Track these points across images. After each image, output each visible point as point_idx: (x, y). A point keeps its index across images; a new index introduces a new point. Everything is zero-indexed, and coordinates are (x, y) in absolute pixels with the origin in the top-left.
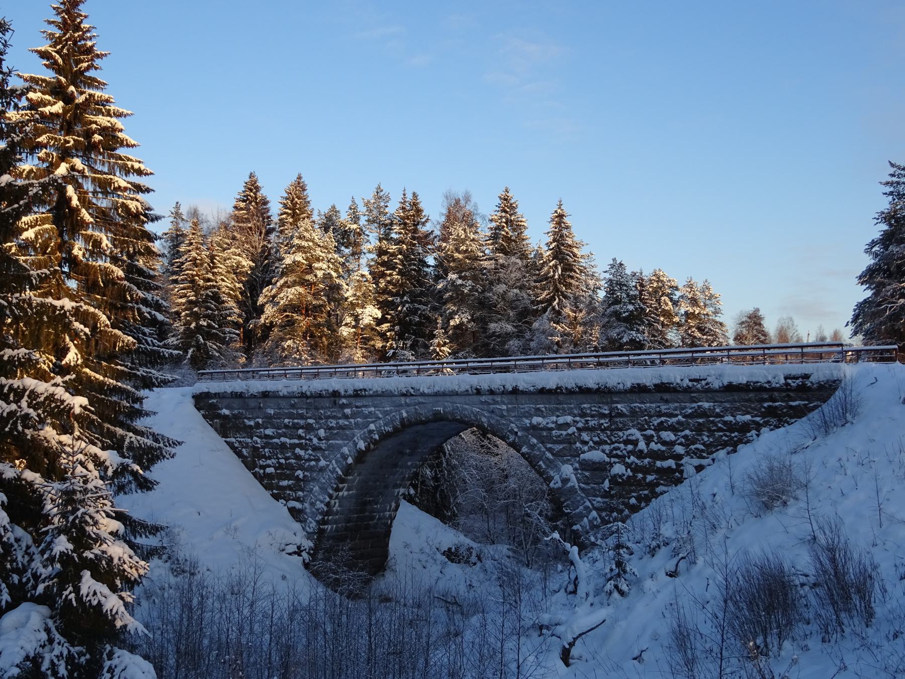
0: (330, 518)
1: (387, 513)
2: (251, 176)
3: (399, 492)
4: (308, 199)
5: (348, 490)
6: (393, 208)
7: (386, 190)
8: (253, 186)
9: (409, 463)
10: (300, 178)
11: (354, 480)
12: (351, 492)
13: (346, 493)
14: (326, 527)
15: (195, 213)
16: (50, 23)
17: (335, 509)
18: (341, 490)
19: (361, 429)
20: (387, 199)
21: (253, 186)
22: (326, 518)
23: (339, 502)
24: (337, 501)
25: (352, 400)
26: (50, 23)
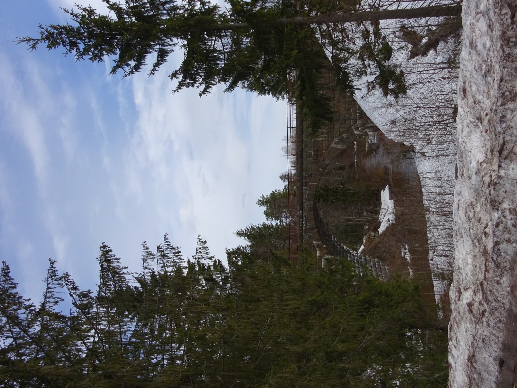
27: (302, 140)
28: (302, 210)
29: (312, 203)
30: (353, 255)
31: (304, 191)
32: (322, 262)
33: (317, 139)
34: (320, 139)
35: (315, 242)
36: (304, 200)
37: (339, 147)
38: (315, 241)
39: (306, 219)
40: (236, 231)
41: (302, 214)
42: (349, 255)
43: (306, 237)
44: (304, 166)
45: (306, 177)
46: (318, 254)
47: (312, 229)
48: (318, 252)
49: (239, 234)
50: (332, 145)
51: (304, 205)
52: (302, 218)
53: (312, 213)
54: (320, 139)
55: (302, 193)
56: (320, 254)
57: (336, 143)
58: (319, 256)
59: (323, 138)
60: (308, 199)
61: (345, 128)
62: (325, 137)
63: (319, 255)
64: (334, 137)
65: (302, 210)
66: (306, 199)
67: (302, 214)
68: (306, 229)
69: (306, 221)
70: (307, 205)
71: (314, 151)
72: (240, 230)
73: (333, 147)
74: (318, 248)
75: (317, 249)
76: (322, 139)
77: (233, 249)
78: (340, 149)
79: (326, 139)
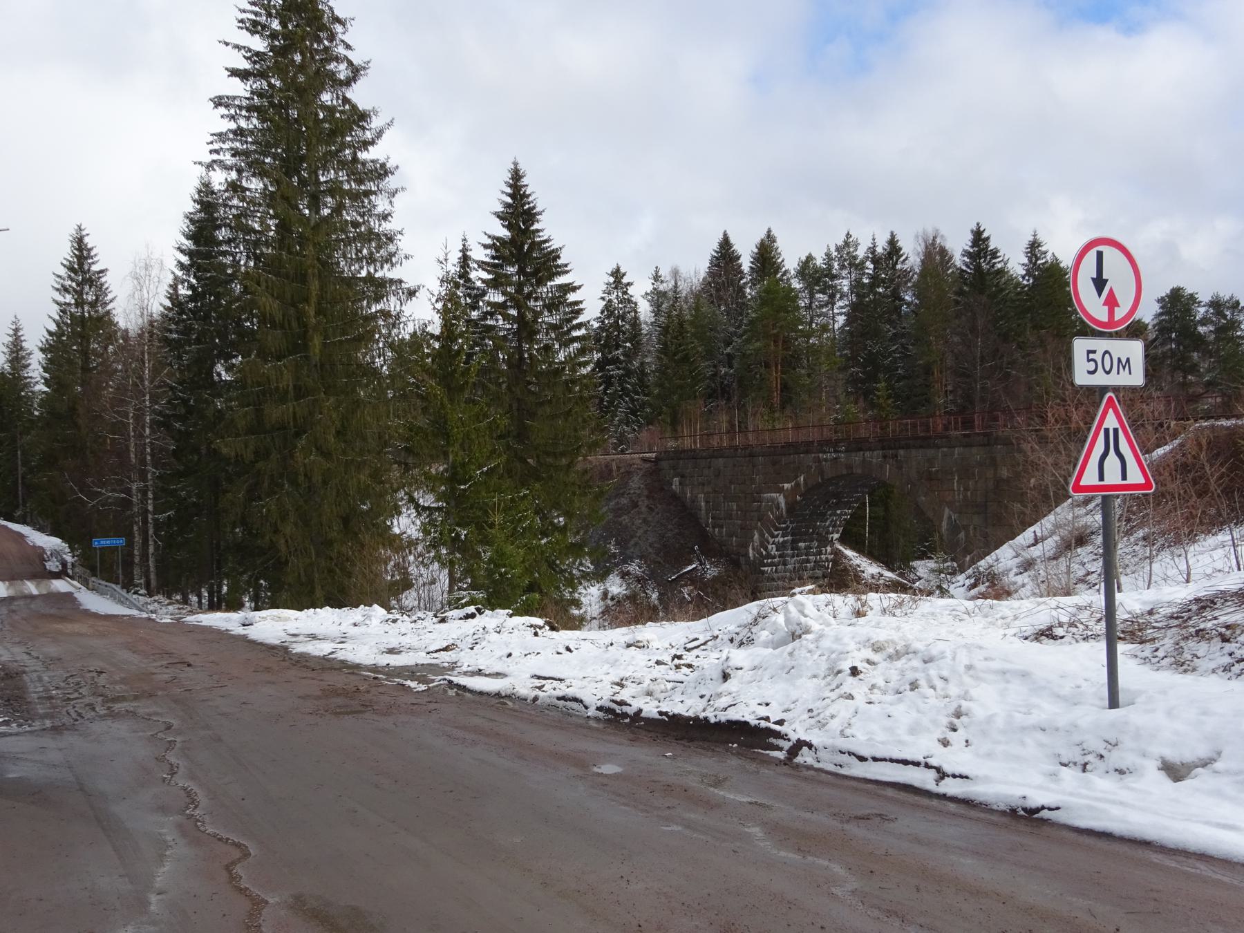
0: (769, 561)
1: (823, 557)
2: (725, 235)
3: (832, 538)
4: (779, 251)
5: (783, 536)
6: (861, 253)
7: (854, 236)
8: (725, 244)
9: (839, 512)
10: (769, 231)
11: (788, 527)
12: (786, 538)
13: (781, 540)
14: (766, 569)
15: (675, 273)
16: (503, 192)
17: (773, 553)
18: (777, 536)
20: (856, 245)
21: (725, 244)
22: (765, 561)
23: (777, 547)
24: (774, 546)
26: (503, 192)
27: (954, 447)
28: (846, 451)
29: (859, 471)
30: (820, 553)
33: (956, 478)
34: (955, 484)
35: (802, 479)
36: (862, 453)
37: (944, 524)
38: (804, 478)
39: (836, 458)
40: (1041, 237)
41: (840, 452)
42: (815, 544)
43: (809, 459)
44: (914, 452)
45: (896, 456)
46: (787, 486)
47: (822, 473)
49: (1034, 246)
50: (947, 511)
51: (853, 454)
52: (836, 451)
53: (845, 472)
54: (955, 484)
55: (873, 451)
56: (787, 489)
57: (950, 517)
59: (959, 490)
61: (975, 536)
62: (959, 495)
63: (785, 488)
64: (960, 513)
65: (846, 451)
66: (864, 458)
67: (840, 452)
68: (819, 461)
69: (831, 460)
70: (855, 460)
71: (937, 471)
72: (1043, 249)
73: (944, 510)
76: (956, 488)
77: (988, 238)
78: (941, 527)
79: (957, 497)
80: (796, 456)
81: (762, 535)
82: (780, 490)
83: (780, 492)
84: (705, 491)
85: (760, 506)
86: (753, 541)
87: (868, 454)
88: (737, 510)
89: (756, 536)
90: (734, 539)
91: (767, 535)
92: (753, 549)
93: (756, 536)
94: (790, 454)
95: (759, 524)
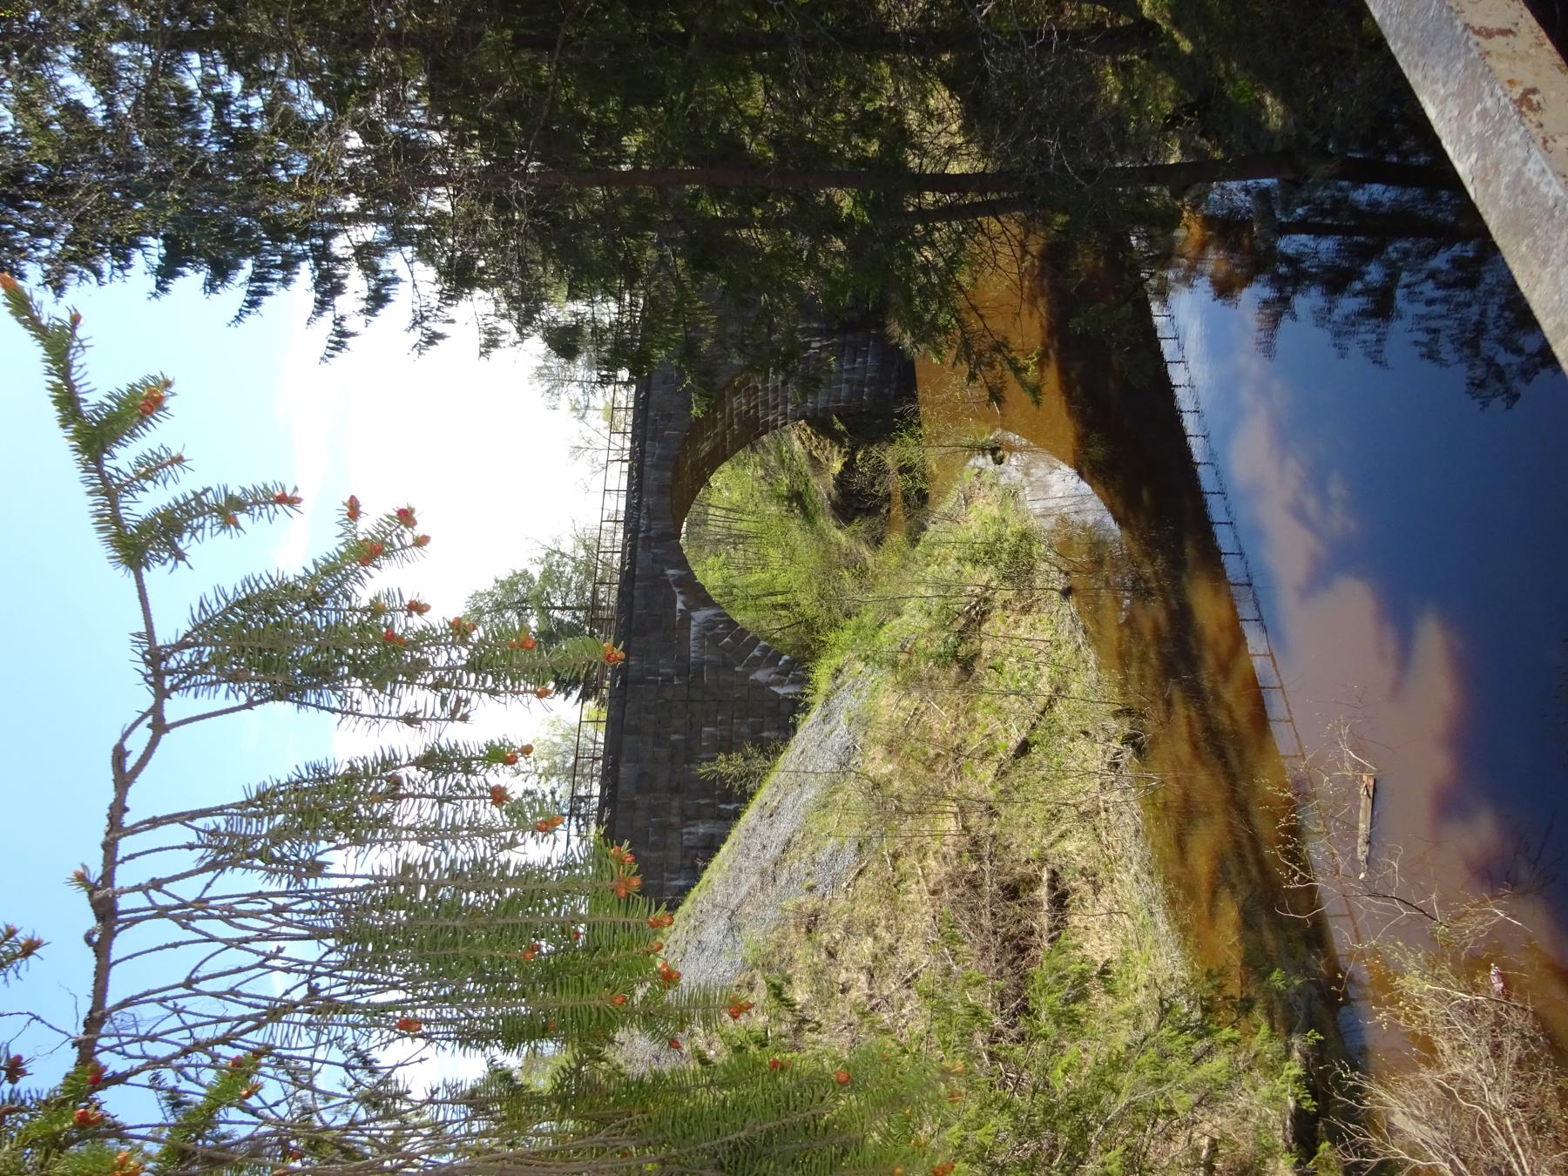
19: (675, 601)
25: (637, 612)
29: (669, 474)
31: (648, 448)
32: (689, 628)
35: (671, 572)
44: (653, 398)
46: (679, 606)
48: (680, 598)
56: (683, 602)
58: (681, 610)
60: (656, 466)
63: (683, 607)
66: (651, 466)
67: (640, 499)
68: (648, 538)
74: (678, 586)
75: (677, 590)
80: (637, 584)
81: (756, 664)
82: (686, 618)
83: (690, 618)
84: (675, 820)
85: (708, 662)
86: (769, 684)
87: (648, 461)
88: (715, 724)
89: (761, 675)
90: (765, 734)
91: (756, 652)
92: (781, 683)
93: (761, 675)
94: (633, 597)
95: (737, 669)
